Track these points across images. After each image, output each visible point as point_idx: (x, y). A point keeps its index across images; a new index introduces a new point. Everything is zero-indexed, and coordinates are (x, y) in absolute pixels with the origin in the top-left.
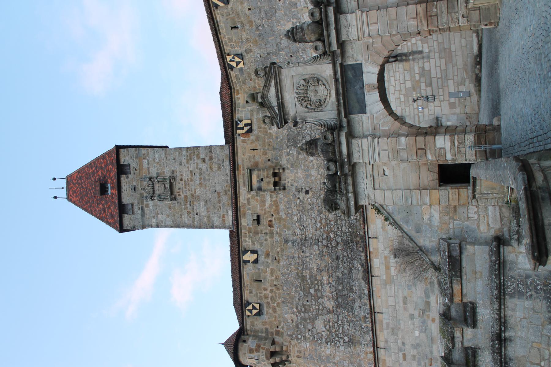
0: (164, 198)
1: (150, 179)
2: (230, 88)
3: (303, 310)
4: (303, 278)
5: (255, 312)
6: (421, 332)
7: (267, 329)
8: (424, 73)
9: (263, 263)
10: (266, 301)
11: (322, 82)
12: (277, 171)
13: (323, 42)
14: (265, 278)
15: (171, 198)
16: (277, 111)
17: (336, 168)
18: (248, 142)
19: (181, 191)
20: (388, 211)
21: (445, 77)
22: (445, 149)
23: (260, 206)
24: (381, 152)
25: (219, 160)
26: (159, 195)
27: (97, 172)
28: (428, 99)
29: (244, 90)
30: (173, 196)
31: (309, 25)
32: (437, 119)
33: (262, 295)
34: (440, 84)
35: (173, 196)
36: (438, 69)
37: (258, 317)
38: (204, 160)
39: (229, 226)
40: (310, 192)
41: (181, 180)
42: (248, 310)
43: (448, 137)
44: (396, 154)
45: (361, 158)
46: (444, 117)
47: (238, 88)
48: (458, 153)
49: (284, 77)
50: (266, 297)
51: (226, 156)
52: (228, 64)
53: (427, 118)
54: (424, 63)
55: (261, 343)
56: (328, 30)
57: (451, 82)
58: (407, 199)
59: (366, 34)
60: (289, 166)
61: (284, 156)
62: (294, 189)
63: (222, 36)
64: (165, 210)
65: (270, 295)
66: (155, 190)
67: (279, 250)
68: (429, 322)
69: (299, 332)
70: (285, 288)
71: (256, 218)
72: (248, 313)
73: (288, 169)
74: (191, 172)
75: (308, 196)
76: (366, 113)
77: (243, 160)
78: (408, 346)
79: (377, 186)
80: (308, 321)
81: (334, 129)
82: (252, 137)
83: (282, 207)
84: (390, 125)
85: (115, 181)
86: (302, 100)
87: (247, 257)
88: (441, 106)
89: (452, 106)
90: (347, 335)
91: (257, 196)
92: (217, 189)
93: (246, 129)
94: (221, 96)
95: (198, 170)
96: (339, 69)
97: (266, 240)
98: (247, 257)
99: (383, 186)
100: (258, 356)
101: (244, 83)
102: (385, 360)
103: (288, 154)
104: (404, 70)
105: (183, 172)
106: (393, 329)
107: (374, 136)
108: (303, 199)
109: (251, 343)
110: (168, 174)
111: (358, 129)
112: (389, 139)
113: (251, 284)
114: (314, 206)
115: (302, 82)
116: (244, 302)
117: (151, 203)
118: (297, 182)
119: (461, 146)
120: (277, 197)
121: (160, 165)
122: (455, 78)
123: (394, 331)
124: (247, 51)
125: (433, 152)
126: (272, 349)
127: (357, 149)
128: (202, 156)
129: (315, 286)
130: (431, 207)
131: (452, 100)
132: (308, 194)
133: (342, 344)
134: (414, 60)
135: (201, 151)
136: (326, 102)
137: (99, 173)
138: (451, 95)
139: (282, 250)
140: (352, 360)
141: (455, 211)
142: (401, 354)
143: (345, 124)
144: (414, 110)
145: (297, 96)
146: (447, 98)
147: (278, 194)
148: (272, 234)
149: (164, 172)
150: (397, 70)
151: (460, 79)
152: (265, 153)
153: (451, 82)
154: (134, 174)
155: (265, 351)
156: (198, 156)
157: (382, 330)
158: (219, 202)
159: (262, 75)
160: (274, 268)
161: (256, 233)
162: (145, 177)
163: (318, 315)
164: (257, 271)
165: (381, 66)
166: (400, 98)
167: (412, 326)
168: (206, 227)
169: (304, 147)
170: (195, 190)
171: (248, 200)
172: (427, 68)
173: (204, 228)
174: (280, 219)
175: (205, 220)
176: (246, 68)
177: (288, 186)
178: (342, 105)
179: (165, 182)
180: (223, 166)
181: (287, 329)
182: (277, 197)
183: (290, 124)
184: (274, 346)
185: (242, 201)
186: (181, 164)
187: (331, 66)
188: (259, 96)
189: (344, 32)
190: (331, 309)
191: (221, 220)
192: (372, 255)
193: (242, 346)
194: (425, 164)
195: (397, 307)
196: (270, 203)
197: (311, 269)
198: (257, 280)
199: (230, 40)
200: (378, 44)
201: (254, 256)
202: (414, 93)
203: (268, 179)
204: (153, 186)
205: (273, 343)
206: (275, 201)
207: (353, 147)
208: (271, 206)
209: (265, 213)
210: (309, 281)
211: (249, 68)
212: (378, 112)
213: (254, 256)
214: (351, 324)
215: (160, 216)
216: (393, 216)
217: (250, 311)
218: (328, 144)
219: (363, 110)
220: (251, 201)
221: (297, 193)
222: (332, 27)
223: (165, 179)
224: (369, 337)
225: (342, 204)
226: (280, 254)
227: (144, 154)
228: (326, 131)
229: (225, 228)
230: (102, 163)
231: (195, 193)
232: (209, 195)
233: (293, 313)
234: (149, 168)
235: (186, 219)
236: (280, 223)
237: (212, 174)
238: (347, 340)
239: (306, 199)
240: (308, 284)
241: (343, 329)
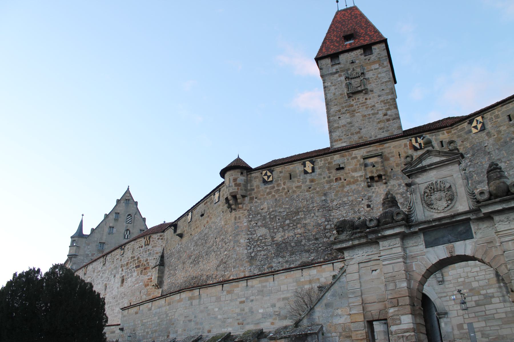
0: (348, 88)
1: (363, 73)
2: (452, 125)
3: (272, 217)
4: (297, 213)
5: (266, 178)
6: (263, 314)
7: (253, 189)
8: (488, 298)
9: (305, 178)
10: (275, 186)
11: (451, 204)
12: (383, 177)
13: (489, 199)
14: (293, 182)
15: (349, 93)
16: (418, 167)
17: (373, 227)
18: (405, 149)
19: (357, 100)
20: (341, 277)
21: (487, 318)
22: (400, 324)
23: (351, 169)
24: (391, 266)
25: (388, 127)
26: (350, 84)
27: (363, 29)
28: (463, 303)
29: (452, 137)
30: (351, 95)
31: (504, 183)
32: (446, 314)
33: (279, 182)
34: (480, 314)
35: (353, 94)
36: (494, 311)
37: (262, 181)
38: (385, 115)
39: (333, 146)
40: (369, 209)
41: (366, 99)
42: (266, 173)
43: (411, 326)
44: (391, 279)
45: (384, 248)
46: (448, 320)
47: (453, 132)
48: (398, 337)
49: (450, 167)
50: (278, 185)
51: (392, 133)
52: (473, 119)
53: (445, 304)
54: (498, 297)
55: (242, 187)
56: (501, 202)
57: (483, 324)
58: (353, 293)
59: (503, 239)
60: (389, 187)
61: (398, 182)
62: (370, 194)
63: (500, 108)
64: (339, 91)
65: (281, 188)
66: (355, 79)
67: (318, 189)
68: (271, 320)
69: (254, 215)
70: (287, 199)
71: (341, 166)
72: (264, 172)
73: (387, 187)
74: (374, 106)
75: (366, 207)
76: (426, 248)
77: (389, 147)
78: (250, 304)
79: (361, 265)
80: (264, 222)
81: (408, 220)
82: (410, 152)
83: (354, 187)
84: (417, 271)
85: (357, 45)
86: (431, 188)
87: (308, 164)
88: (458, 316)
89: (460, 327)
90: (256, 255)
91: (360, 164)
92: (362, 130)
93: (417, 145)
94: (446, 119)
95: (376, 112)
96: (464, 217)
97: (324, 178)
98: (308, 164)
99: (363, 271)
100: (232, 186)
101: (459, 136)
102: (238, 287)
103: (400, 185)
104: (488, 279)
105: (373, 100)
106: (262, 291)
107: (405, 257)
108: (363, 204)
109: (241, 179)
110: (369, 87)
111: (410, 242)
112: (404, 272)
113: (287, 171)
114: (358, 214)
115: (448, 185)
116: (272, 168)
117: (343, 78)
118: (376, 197)
119: (405, 338)
120: (361, 181)
121: (376, 79)
122: (488, 328)
123: (261, 292)
124: (489, 134)
125: (396, 313)
126: (238, 196)
127: (392, 244)
128: (389, 113)
129: (292, 223)
130: (348, 315)
131: (465, 326)
132: (368, 207)
133: (249, 251)
134: (500, 287)
135: (394, 111)
136: (432, 210)
137: (362, 31)
138: (470, 325)
139: (317, 192)
140: (238, 261)
141: (347, 337)
142: (244, 299)
143: (412, 230)
144: (451, 291)
145: (434, 182)
146: (467, 321)
147: (364, 182)
148: (329, 182)
149: (371, 83)
150: (487, 273)
151: (487, 332)
152: (397, 165)
153: (483, 324)
154: (365, 59)
155: (236, 190)
156: (388, 109)
157: (260, 282)
158: (352, 134)
159: (450, 147)
160: (303, 188)
161: (329, 169)
162: (364, 69)
163: (269, 229)
164: (298, 174)
165: (473, 256)
166: (461, 277)
167: (266, 306)
168: (330, 127)
169: (389, 196)
170: (359, 112)
171: (356, 157)
172: (493, 300)
173: (329, 126)
174: (343, 186)
175: (336, 125)
176: (473, 135)
177: (372, 189)
178: (431, 225)
179: (363, 86)
180: (383, 132)
181: (255, 206)
182: (361, 181)
183: (409, 181)
184: (241, 197)
185: (354, 152)
186: (379, 96)
187: (467, 209)
188: (430, 148)
189: (503, 217)
190: (275, 239)
191: (337, 138)
192: (319, 267)
193: (238, 172)
194: (386, 307)
195: (280, 293)
196: (356, 176)
197: (305, 218)
198: (291, 175)
199: (497, 117)
200: (495, 252)
201: (310, 171)
202: (468, 291)
203: (375, 171)
204: (357, 77)
205: (244, 197)
206: (357, 180)
207: (393, 240)
208: (353, 177)
209: (346, 174)
210: (295, 218)
211: (473, 138)
212: (429, 259)
213: (310, 171)
214: (265, 257)
215: (333, 88)
216: (338, 282)
217: (266, 174)
218: (393, 217)
219: (428, 245)
220: (355, 160)
221: (366, 197)
222: (505, 206)
223: (364, 86)
224: (256, 272)
225: (343, 237)
226: (314, 191)
227: (383, 64)
228: (404, 213)
229: (331, 142)
230: (370, 31)
231: (357, 113)
232: (357, 125)
233: (269, 209)
234: (372, 70)
235: (334, 109)
236: (340, 187)
237: (375, 124)
238: (253, 255)
239: (362, 206)
240: (293, 218)
241: (260, 251)
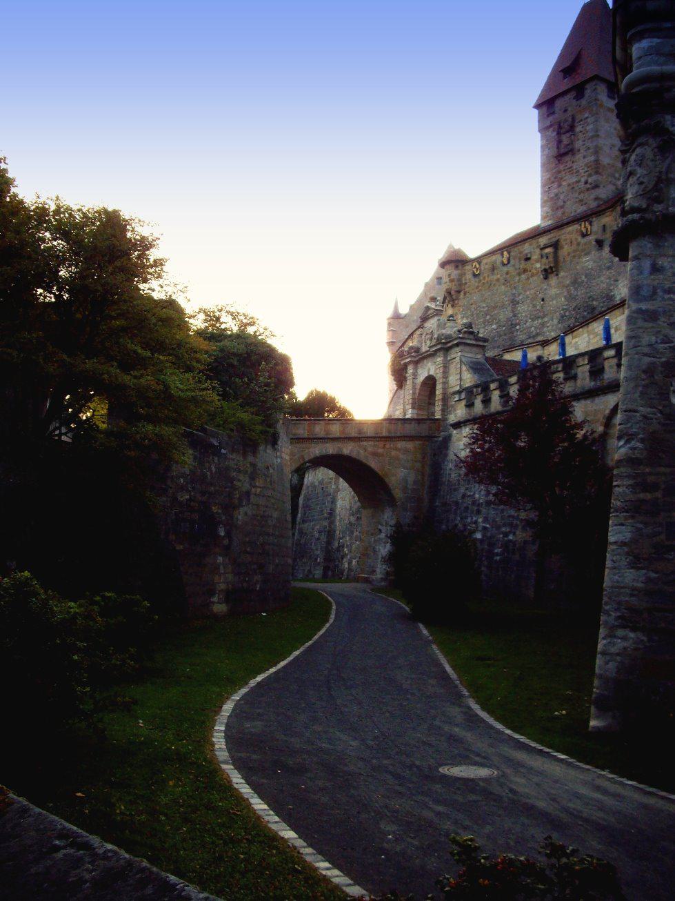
38: (586, 183)
128: (590, 181)
156: (590, 175)
186: (584, 157)
201: (505, 262)
205: (459, 292)
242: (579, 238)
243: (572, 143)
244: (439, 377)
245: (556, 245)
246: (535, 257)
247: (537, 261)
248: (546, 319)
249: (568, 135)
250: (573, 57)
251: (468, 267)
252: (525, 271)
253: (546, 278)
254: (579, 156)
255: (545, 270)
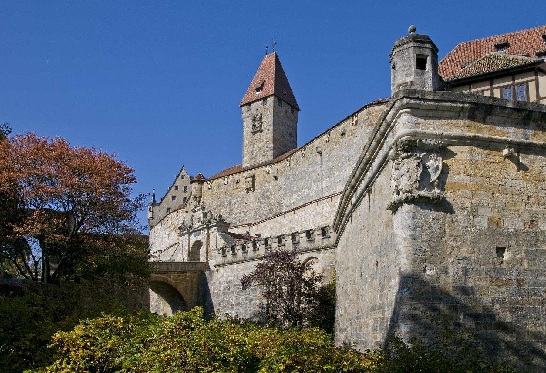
4: (220, 206)
38: (267, 147)
156: (269, 144)
242: (265, 174)
243: (261, 126)
244: (204, 241)
245: (253, 177)
246: (241, 182)
247: (243, 184)
248: (248, 213)
249: (259, 122)
250: (261, 84)
251: (205, 184)
252: (237, 188)
253: (248, 193)
254: (263, 133)
255: (247, 189)
